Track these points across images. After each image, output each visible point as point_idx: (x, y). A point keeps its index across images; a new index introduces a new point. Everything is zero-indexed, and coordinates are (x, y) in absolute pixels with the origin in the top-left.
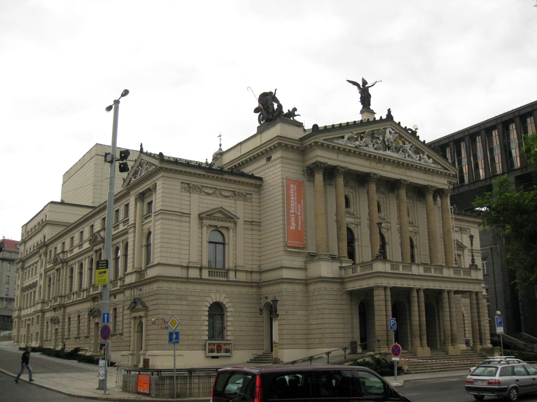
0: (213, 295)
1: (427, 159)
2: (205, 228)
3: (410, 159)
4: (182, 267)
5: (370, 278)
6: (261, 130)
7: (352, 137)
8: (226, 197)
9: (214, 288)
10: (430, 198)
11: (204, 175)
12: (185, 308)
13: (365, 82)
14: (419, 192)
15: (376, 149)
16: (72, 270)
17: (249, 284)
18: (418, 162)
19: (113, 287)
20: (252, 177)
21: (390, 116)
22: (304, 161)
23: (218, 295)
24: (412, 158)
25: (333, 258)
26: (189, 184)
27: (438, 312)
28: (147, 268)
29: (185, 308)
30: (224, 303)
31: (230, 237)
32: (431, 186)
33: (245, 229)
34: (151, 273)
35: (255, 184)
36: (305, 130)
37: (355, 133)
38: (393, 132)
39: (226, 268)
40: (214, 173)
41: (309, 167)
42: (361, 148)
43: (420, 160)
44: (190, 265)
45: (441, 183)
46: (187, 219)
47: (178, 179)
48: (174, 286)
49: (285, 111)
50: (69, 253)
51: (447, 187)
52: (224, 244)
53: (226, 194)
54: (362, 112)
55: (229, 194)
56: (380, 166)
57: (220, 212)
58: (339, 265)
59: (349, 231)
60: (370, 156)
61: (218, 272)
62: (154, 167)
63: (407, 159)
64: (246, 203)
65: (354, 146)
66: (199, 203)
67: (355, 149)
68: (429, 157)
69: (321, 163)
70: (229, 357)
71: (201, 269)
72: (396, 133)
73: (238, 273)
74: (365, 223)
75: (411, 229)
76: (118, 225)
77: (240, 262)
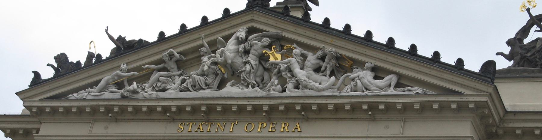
3: (299, 93)
24: (306, 87)
37: (124, 66)
42: (140, 96)
63: (288, 93)
65: (118, 96)
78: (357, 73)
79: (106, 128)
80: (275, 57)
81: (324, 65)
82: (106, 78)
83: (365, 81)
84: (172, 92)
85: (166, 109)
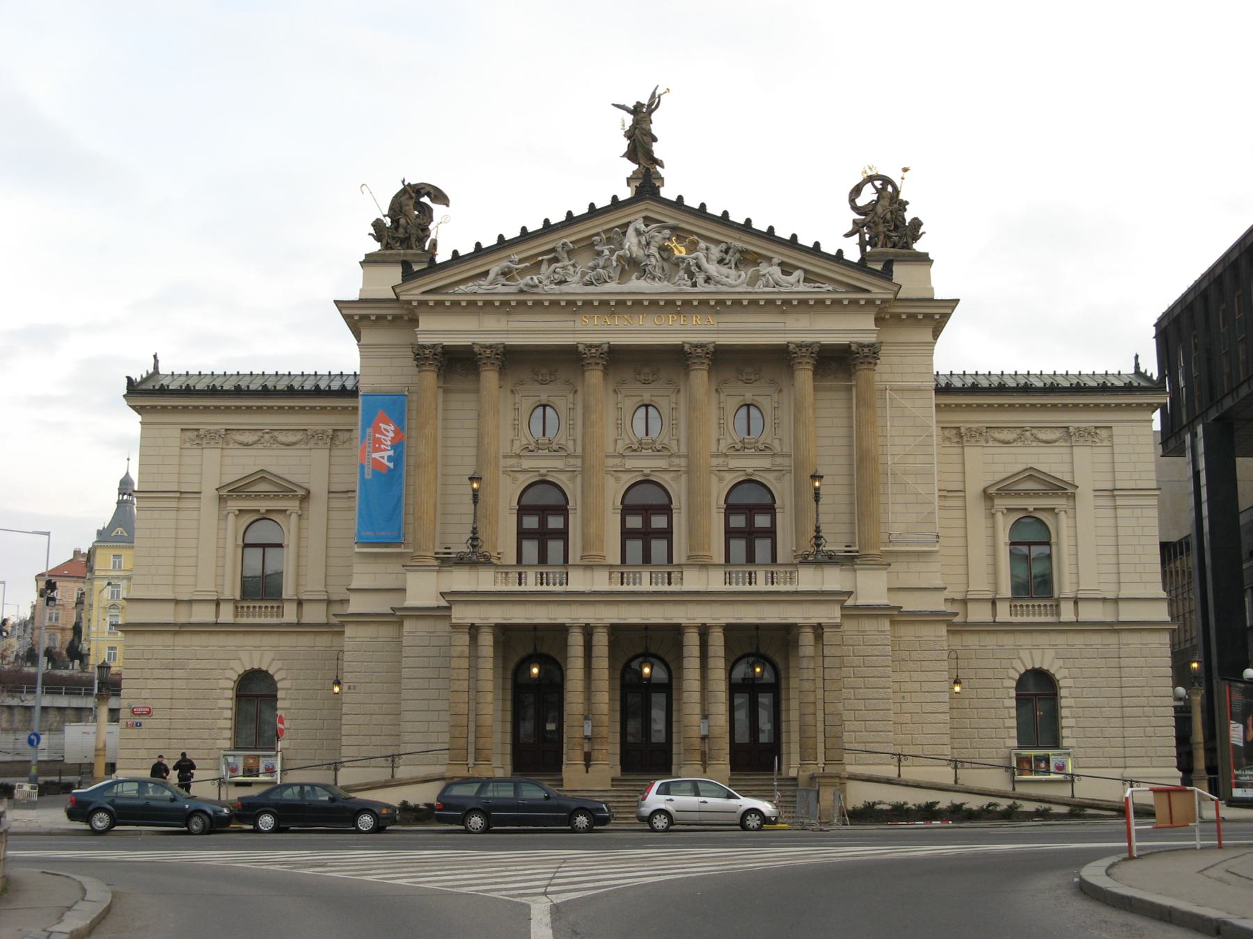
2: (231, 517)
12: (178, 684)
23: (256, 655)
27: (788, 678)
29: (178, 684)
32: (800, 346)
37: (516, 258)
46: (194, 504)
53: (291, 438)
56: (619, 322)
65: (513, 289)
69: (423, 347)
73: (306, 607)
78: (764, 268)
79: (498, 321)
80: (680, 251)
81: (728, 258)
82: (495, 270)
83: (776, 277)
84: (575, 287)
85: (571, 303)
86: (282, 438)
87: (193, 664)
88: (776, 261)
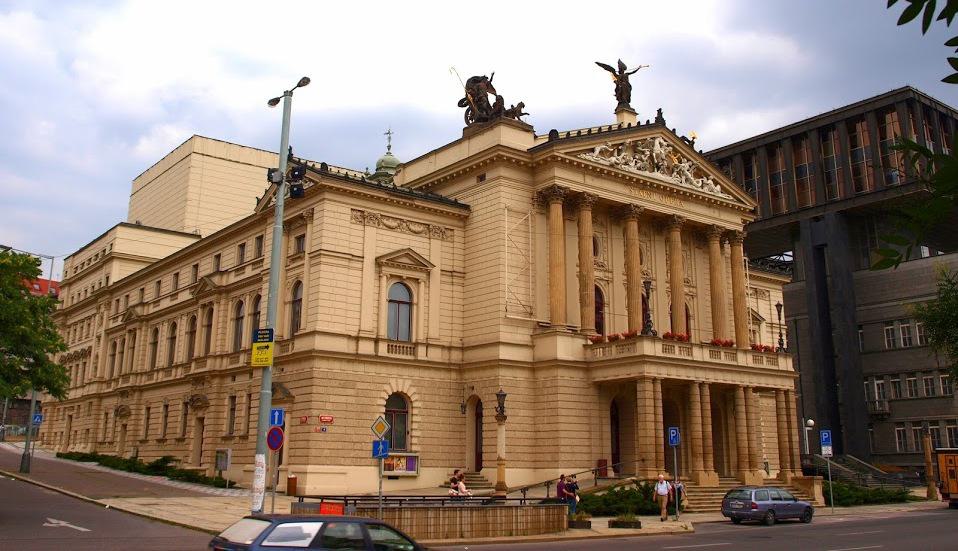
0: (393, 382)
1: (713, 186)
4: (349, 337)
5: (631, 364)
6: (469, 134)
7: (607, 151)
8: (415, 232)
9: (395, 371)
10: (716, 246)
11: (386, 199)
12: (351, 400)
13: (622, 67)
14: (699, 235)
15: (639, 169)
16: (156, 331)
17: (446, 367)
18: (700, 190)
19: (231, 363)
20: (455, 204)
21: (660, 120)
22: (534, 184)
23: (400, 381)
24: (691, 183)
25: (573, 332)
26: (363, 212)
28: (293, 338)
29: (351, 400)
30: (409, 395)
31: (420, 294)
32: (718, 227)
33: (442, 282)
34: (300, 345)
35: (460, 215)
36: (536, 137)
37: (610, 144)
38: (665, 143)
39: (414, 340)
40: (401, 197)
41: (541, 193)
43: (702, 187)
44: (361, 335)
45: (733, 222)
46: (359, 265)
47: (348, 204)
48: (336, 366)
49: (507, 107)
50: (152, 306)
51: (741, 229)
52: (410, 304)
54: (618, 111)
55: (421, 228)
56: (644, 194)
57: (407, 255)
58: (583, 342)
59: (598, 290)
60: (631, 178)
61: (402, 344)
62: (312, 184)
63: (683, 185)
64: (445, 244)
65: (608, 164)
66: (380, 241)
67: (611, 169)
68: (716, 183)
69: (559, 187)
70: (415, 477)
71: (377, 341)
72: (668, 146)
74: (619, 278)
75: (686, 290)
76: (244, 268)
77: (434, 333)
86: (412, 227)
87: (359, 386)
88: (712, 177)
